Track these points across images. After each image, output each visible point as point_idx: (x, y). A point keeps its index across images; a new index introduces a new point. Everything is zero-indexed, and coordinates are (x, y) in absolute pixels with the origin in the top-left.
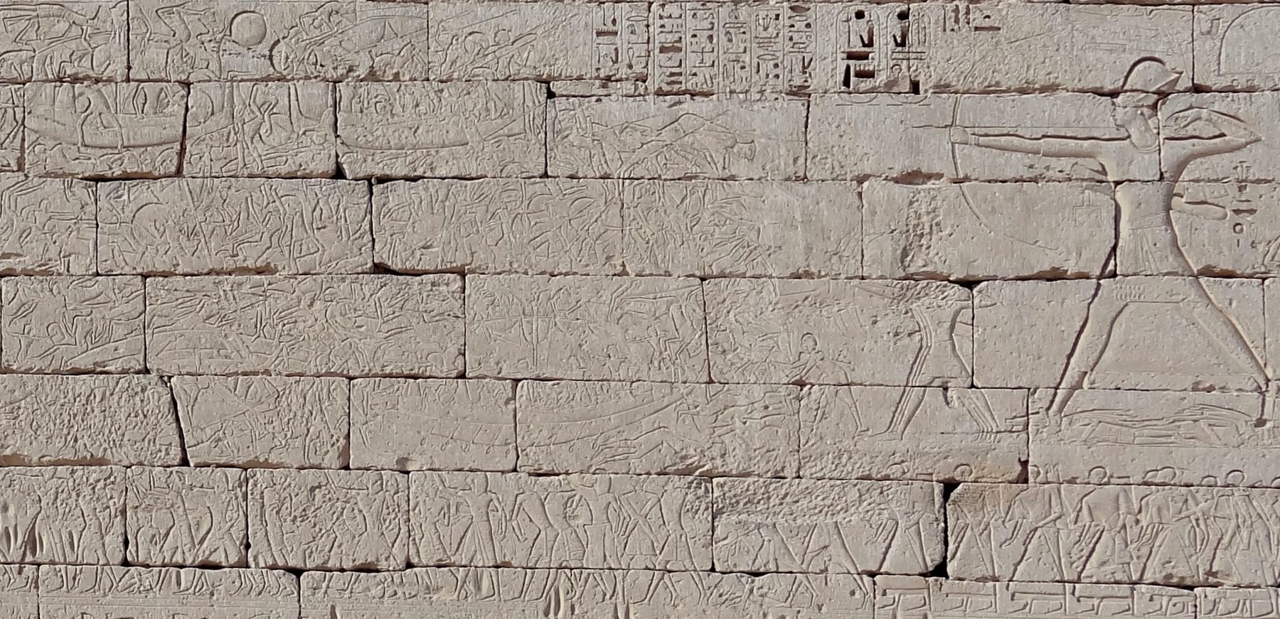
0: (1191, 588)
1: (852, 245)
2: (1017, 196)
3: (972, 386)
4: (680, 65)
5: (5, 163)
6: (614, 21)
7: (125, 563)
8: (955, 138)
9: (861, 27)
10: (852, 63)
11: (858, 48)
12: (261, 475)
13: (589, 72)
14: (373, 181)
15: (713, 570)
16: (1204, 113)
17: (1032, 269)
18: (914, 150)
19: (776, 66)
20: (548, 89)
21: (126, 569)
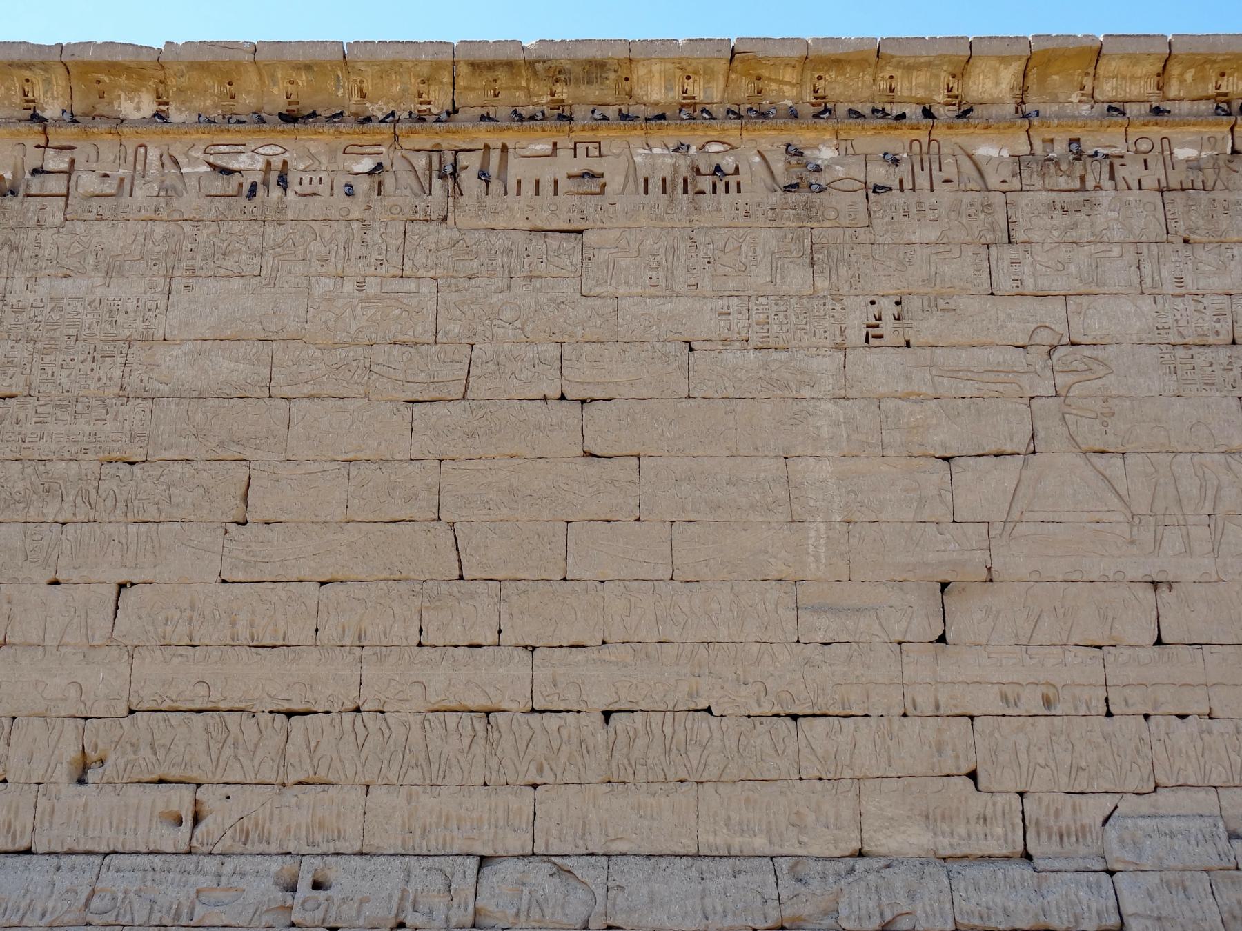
0: (1100, 647)
1: (876, 436)
2: (972, 406)
3: (954, 521)
4: (768, 332)
5: (357, 392)
6: (728, 307)
7: (420, 645)
8: (934, 372)
9: (874, 310)
10: (870, 330)
11: (875, 322)
12: (510, 587)
13: (714, 336)
14: (583, 402)
15: (798, 641)
16: (1078, 357)
17: (985, 449)
18: (909, 379)
19: (825, 332)
20: (690, 346)
21: (420, 648)
